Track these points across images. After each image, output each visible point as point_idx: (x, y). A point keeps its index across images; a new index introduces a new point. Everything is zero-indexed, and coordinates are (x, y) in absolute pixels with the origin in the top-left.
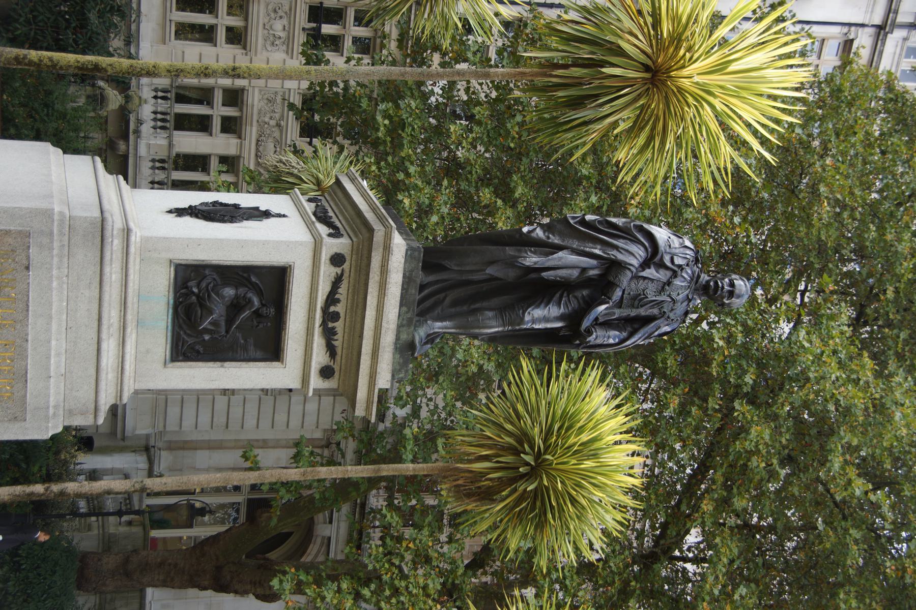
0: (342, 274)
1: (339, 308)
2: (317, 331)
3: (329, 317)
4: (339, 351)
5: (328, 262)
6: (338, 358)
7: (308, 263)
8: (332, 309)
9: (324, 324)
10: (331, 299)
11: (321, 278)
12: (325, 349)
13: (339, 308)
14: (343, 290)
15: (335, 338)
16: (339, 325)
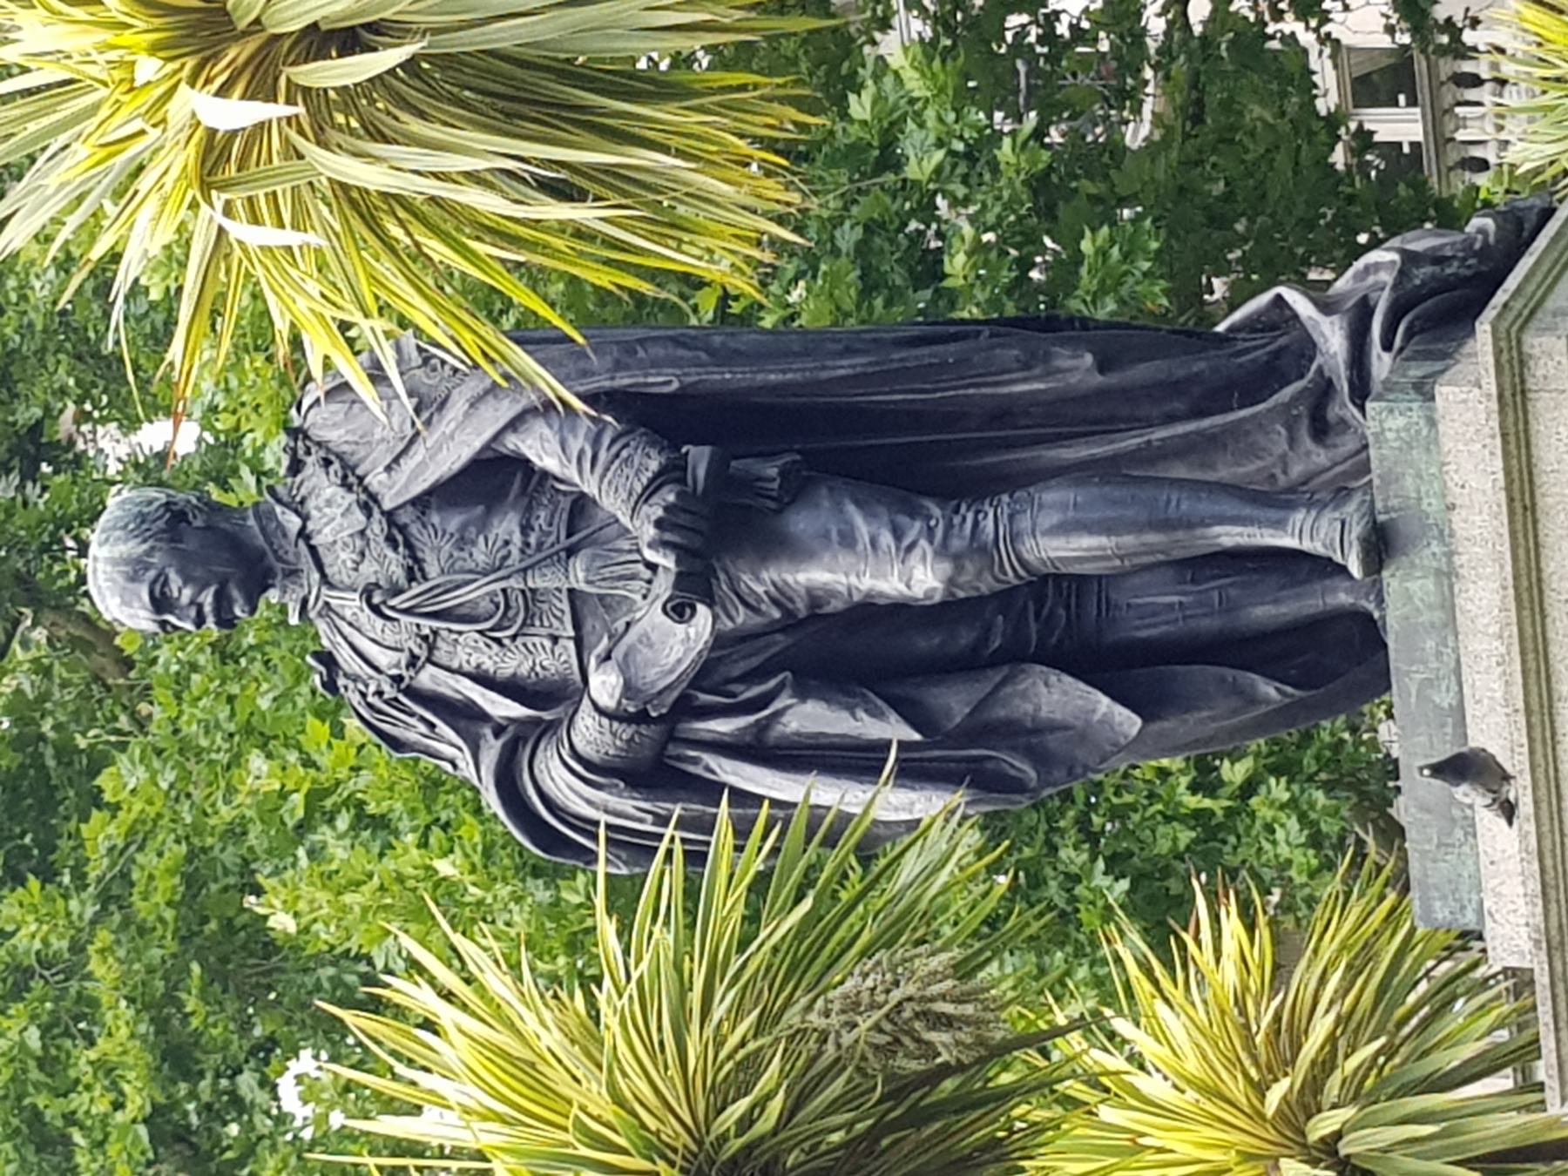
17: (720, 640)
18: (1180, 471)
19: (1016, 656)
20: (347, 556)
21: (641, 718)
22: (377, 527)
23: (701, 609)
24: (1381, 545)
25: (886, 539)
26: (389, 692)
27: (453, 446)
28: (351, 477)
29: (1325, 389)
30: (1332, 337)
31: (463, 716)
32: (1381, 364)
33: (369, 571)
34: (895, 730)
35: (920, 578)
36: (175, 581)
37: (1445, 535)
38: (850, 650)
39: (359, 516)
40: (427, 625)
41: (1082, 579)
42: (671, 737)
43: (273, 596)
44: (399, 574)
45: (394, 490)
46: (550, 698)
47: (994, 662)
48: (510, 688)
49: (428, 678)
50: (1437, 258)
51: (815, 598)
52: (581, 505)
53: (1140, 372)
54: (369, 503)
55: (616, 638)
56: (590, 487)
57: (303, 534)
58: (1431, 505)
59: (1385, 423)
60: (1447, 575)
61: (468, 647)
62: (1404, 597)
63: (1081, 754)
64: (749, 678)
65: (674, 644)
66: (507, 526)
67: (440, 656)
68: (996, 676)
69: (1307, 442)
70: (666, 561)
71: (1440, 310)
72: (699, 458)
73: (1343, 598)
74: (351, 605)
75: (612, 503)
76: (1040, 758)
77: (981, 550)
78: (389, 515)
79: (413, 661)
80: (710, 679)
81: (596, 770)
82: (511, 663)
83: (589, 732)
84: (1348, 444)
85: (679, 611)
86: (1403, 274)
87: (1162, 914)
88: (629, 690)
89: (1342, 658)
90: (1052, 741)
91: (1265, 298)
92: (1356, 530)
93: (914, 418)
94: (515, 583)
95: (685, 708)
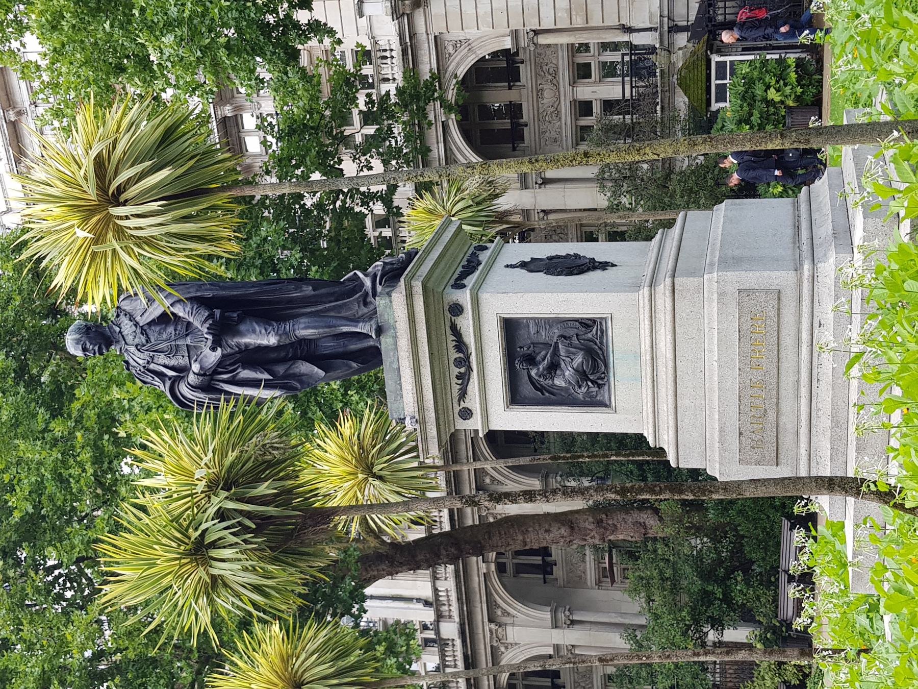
1: (455, 371)
2: (472, 349)
3: (464, 362)
4: (449, 331)
5: (474, 412)
6: (448, 324)
7: (491, 411)
8: (463, 370)
10: (464, 378)
12: (462, 332)
13: (455, 371)
14: (456, 389)
15: (454, 343)
16: (454, 355)
17: (223, 356)
18: (332, 314)
19: (295, 358)
20: (131, 337)
21: (204, 375)
22: (139, 330)
23: (219, 349)
24: (380, 331)
25: (263, 331)
26: (142, 370)
27: (155, 312)
28: (131, 318)
29: (367, 294)
30: (368, 282)
32: (379, 288)
33: (137, 341)
34: (266, 376)
35: (272, 340)
36: (88, 344)
37: (395, 328)
38: (255, 357)
39: (134, 328)
40: (151, 354)
41: (310, 340)
42: (212, 379)
43: (113, 347)
44: (144, 341)
45: (143, 321)
46: (183, 370)
47: (289, 360)
48: (172, 368)
49: (152, 366)
50: (391, 264)
51: (246, 345)
52: (189, 324)
53: (323, 291)
55: (198, 356)
56: (191, 320)
57: (120, 332)
58: (391, 321)
59: (380, 302)
60: (395, 337)
61: (162, 359)
62: (385, 343)
63: (311, 381)
64: (231, 365)
65: (212, 357)
66: (171, 329)
67: (155, 361)
68: (290, 363)
69: (362, 307)
70: (210, 337)
71: (392, 275)
72: (217, 312)
73: (372, 343)
74: (132, 349)
76: (301, 382)
77: (286, 333)
78: (141, 327)
79: (148, 362)
80: (220, 363)
81: (194, 388)
82: (173, 362)
83: (192, 378)
84: (372, 307)
85: (213, 349)
86: (384, 267)
87: (332, 419)
88: (201, 368)
89: (372, 357)
90: (304, 378)
91: (352, 273)
92: (374, 327)
93: (269, 302)
94: (173, 343)
95: (215, 372)
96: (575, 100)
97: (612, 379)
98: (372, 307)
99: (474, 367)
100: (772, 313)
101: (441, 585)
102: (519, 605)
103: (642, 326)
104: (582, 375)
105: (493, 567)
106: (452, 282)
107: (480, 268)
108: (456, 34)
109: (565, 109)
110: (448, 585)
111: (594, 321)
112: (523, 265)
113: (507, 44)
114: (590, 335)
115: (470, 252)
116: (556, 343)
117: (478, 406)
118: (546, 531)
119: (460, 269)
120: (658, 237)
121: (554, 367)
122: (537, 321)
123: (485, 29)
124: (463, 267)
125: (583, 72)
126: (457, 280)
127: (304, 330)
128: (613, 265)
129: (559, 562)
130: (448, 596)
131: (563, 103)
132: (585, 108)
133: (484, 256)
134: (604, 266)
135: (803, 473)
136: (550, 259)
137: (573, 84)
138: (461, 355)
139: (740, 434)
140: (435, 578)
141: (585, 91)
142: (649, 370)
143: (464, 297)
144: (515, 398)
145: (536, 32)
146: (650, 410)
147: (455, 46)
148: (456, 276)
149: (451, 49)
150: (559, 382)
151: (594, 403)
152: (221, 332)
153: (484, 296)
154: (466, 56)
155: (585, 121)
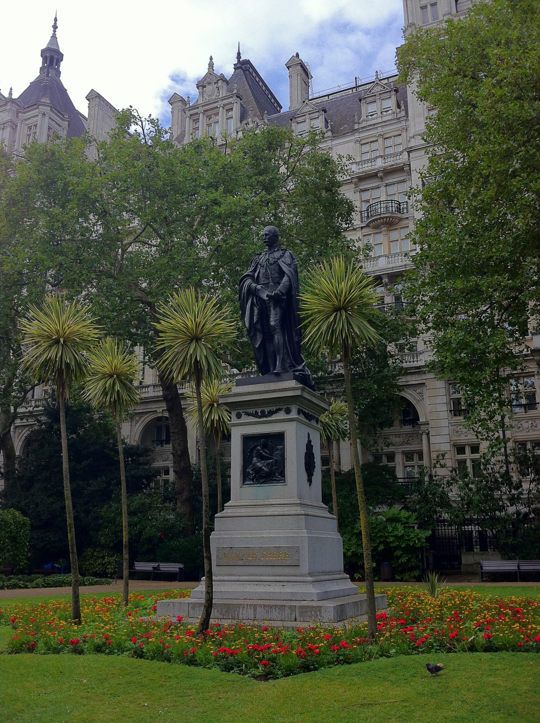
0: (245, 412)
1: (259, 411)
3: (263, 415)
4: (278, 407)
6: (281, 407)
8: (259, 414)
9: (266, 416)
10: (255, 415)
11: (247, 421)
13: (259, 411)
14: (251, 411)
16: (266, 410)
17: (264, 300)
18: (285, 351)
21: (255, 292)
22: (276, 260)
25: (276, 319)
27: (285, 268)
28: (281, 256)
29: (295, 367)
30: (300, 368)
31: (255, 270)
32: (297, 373)
35: (272, 323)
38: (264, 315)
43: (267, 247)
46: (257, 281)
49: (259, 266)
52: (279, 283)
54: (278, 259)
57: (275, 251)
61: (263, 271)
64: (260, 303)
66: (276, 275)
72: (285, 297)
74: (267, 257)
75: (279, 287)
77: (275, 330)
79: (261, 264)
80: (260, 299)
81: (249, 286)
82: (261, 275)
83: (254, 285)
84: (289, 370)
85: (267, 296)
88: (259, 290)
89: (265, 369)
92: (279, 371)
95: (257, 297)
96: (395, 453)
97: (256, 485)
98: (289, 370)
99: (261, 420)
100: (288, 563)
101: (151, 389)
102: (141, 428)
103: (281, 500)
104: (258, 471)
105: (161, 415)
106: (301, 408)
107: (308, 421)
108: (426, 394)
109: (391, 449)
110: (151, 393)
111: (284, 476)
112: (309, 442)
113: (422, 420)
114: (277, 475)
115: (316, 415)
116: (273, 459)
117: (242, 421)
118: (179, 444)
119: (307, 411)
120: (324, 506)
121: (262, 458)
122: (283, 449)
123: (429, 408)
124: (308, 413)
125: (409, 456)
126: (302, 410)
127: (278, 338)
128: (310, 485)
129: (162, 448)
130: (145, 392)
131: (393, 447)
132: (391, 457)
133: (313, 423)
134: (310, 481)
135: (214, 578)
136: (313, 454)
137: (404, 453)
138: (266, 413)
139: (231, 548)
140: (154, 386)
141: (399, 458)
142: (261, 503)
143: (294, 414)
144: (247, 439)
145: (428, 434)
146: (242, 504)
147: (420, 393)
148: (304, 410)
149: (419, 391)
150: (255, 459)
151: (245, 477)
152: (276, 299)
153: (294, 424)
154: (415, 398)
155: (384, 459)
